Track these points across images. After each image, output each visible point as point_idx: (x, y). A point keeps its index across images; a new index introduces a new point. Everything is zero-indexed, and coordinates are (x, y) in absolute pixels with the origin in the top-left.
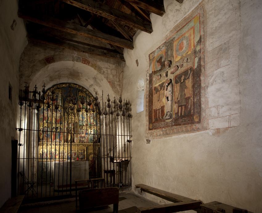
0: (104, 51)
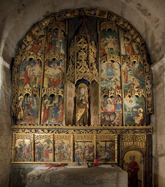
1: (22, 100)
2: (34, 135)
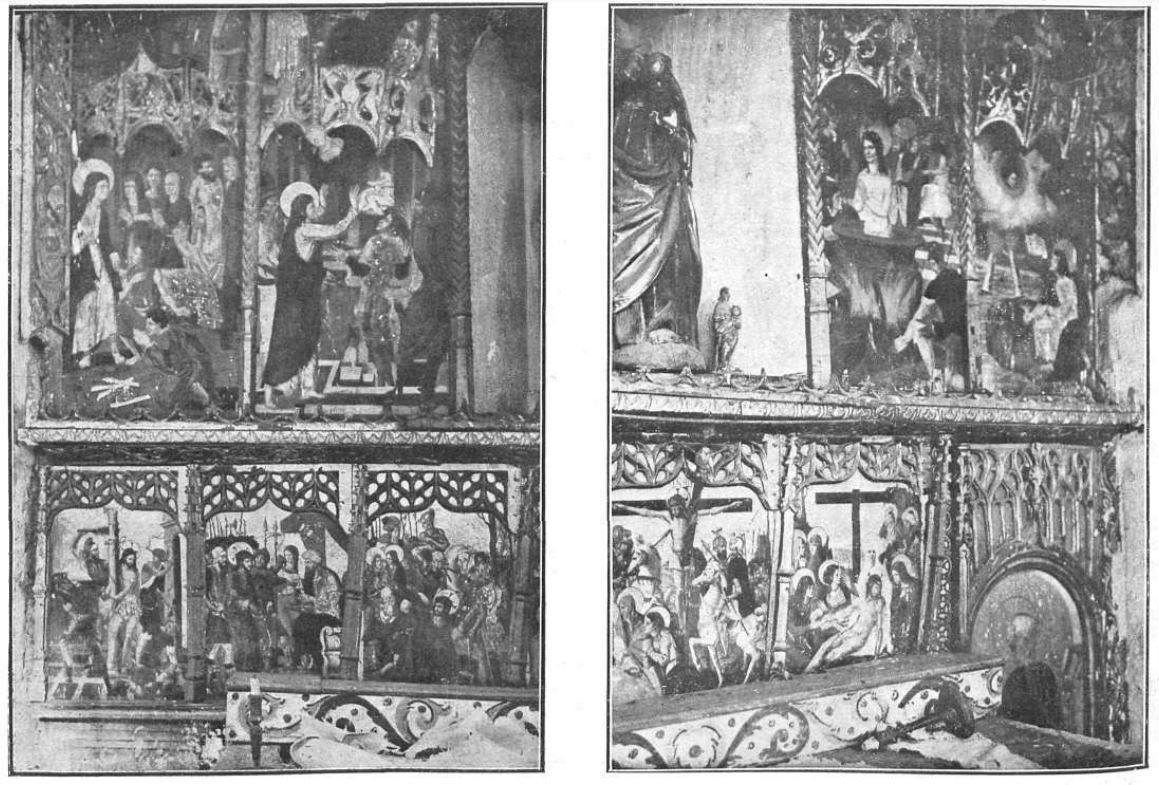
1: (101, 192)
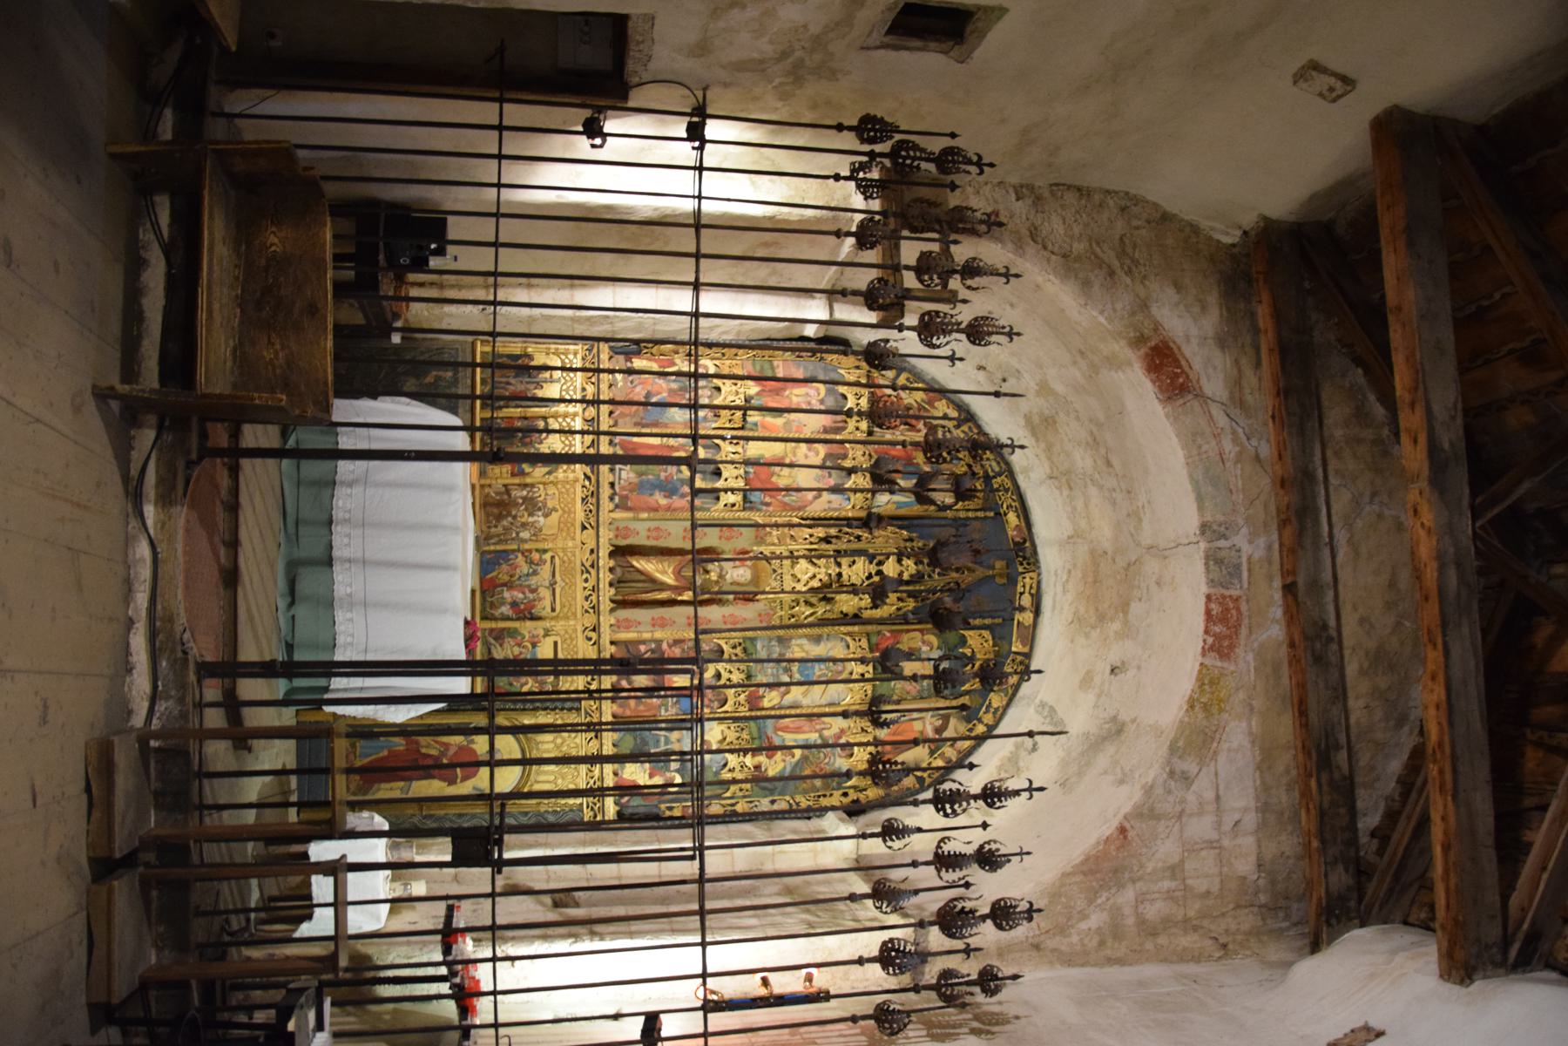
0: (1338, 747)
2: (575, 415)
